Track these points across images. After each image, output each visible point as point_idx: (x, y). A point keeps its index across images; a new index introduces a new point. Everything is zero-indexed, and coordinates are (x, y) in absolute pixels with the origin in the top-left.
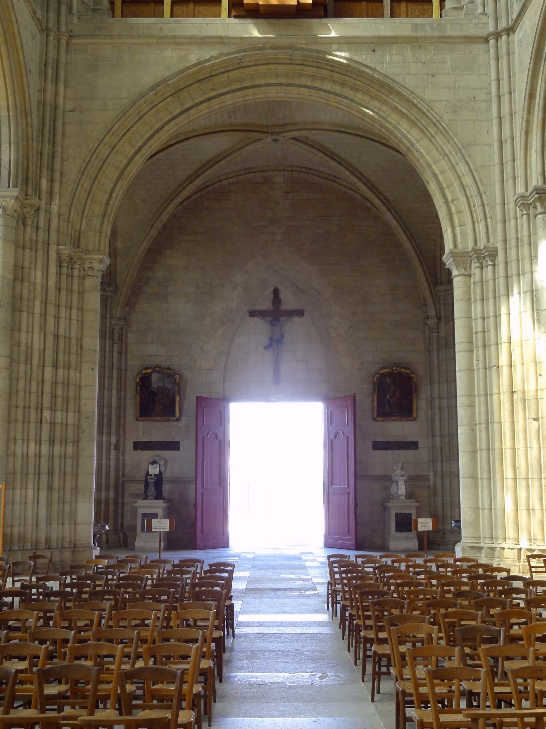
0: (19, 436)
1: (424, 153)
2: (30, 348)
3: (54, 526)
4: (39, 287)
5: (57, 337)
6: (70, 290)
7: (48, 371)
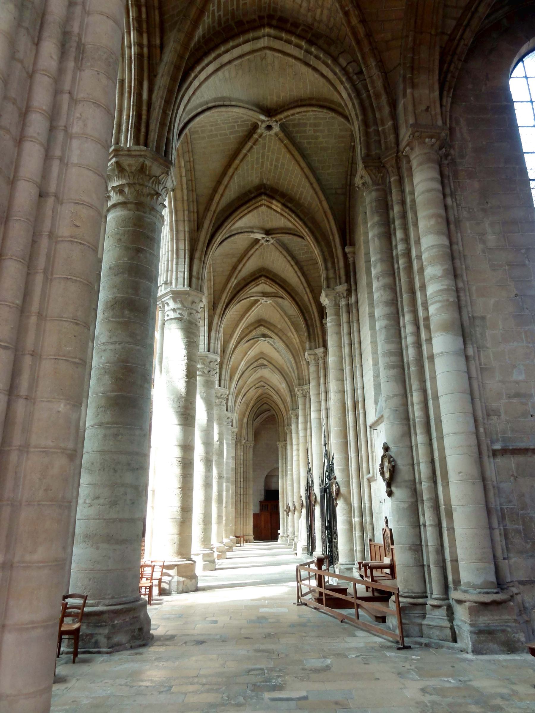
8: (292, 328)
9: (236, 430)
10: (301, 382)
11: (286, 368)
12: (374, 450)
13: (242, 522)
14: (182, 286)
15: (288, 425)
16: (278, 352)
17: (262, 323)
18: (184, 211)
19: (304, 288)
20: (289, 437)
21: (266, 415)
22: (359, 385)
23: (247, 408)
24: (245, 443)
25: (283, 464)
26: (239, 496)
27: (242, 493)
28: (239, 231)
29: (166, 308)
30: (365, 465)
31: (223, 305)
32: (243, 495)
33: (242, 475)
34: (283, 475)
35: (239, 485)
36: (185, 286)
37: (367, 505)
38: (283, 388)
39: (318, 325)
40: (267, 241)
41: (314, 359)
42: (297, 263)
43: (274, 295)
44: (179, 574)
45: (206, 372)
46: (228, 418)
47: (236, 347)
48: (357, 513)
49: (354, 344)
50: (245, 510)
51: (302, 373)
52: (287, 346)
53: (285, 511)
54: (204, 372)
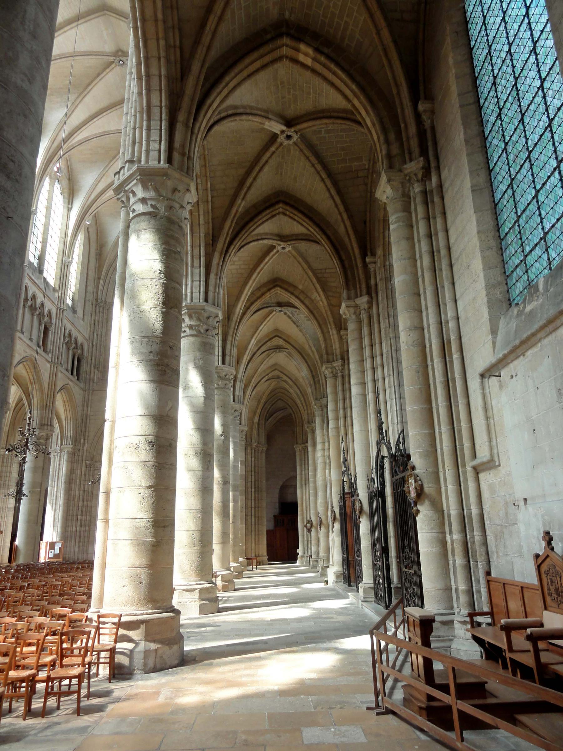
0: (70, 525)
2: (75, 496)
3: (80, 554)
4: (78, 476)
5: (84, 491)
6: (89, 475)
7: (81, 503)
8: (318, 286)
9: (246, 429)
10: (330, 357)
11: (307, 347)
12: (490, 414)
13: (253, 541)
14: (156, 162)
15: (309, 422)
16: (297, 326)
17: (278, 283)
18: (158, 40)
19: (340, 214)
20: (310, 436)
21: (279, 415)
22: (450, 314)
24: (256, 446)
25: (301, 471)
26: (250, 509)
27: (253, 506)
28: (248, 111)
29: (132, 200)
30: (467, 444)
31: (226, 239)
32: (255, 508)
33: (253, 483)
34: (302, 485)
35: (250, 497)
36: (162, 163)
37: (475, 511)
38: (303, 377)
39: (360, 265)
40: (289, 137)
41: (355, 313)
42: (330, 175)
43: (294, 238)
44: (148, 637)
45: (202, 331)
46: (235, 410)
47: (244, 314)
48: (455, 525)
49: (439, 252)
50: (257, 526)
51: (332, 346)
52: (311, 312)
53: (306, 526)
54: (200, 332)
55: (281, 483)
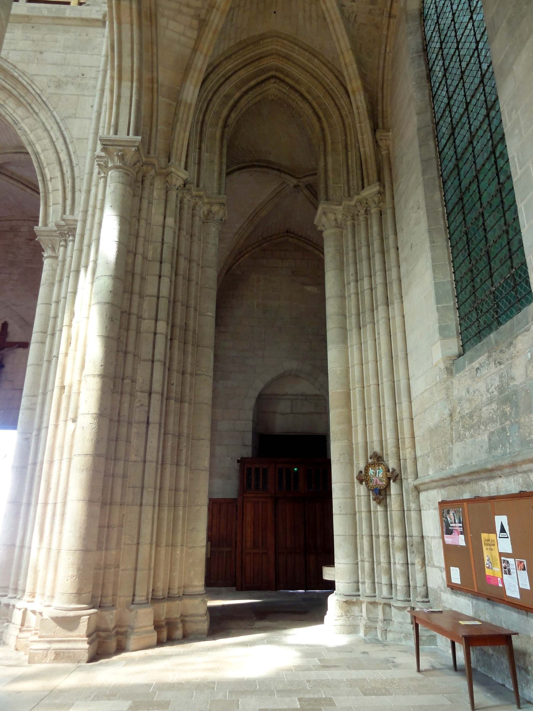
1: (29, 132)
13: (146, 530)
23: (198, 40)
25: (343, 285)
27: (157, 387)
33: (164, 304)
34: (344, 329)
35: (145, 351)
50: (168, 468)
53: (363, 478)
55: (259, 385)
